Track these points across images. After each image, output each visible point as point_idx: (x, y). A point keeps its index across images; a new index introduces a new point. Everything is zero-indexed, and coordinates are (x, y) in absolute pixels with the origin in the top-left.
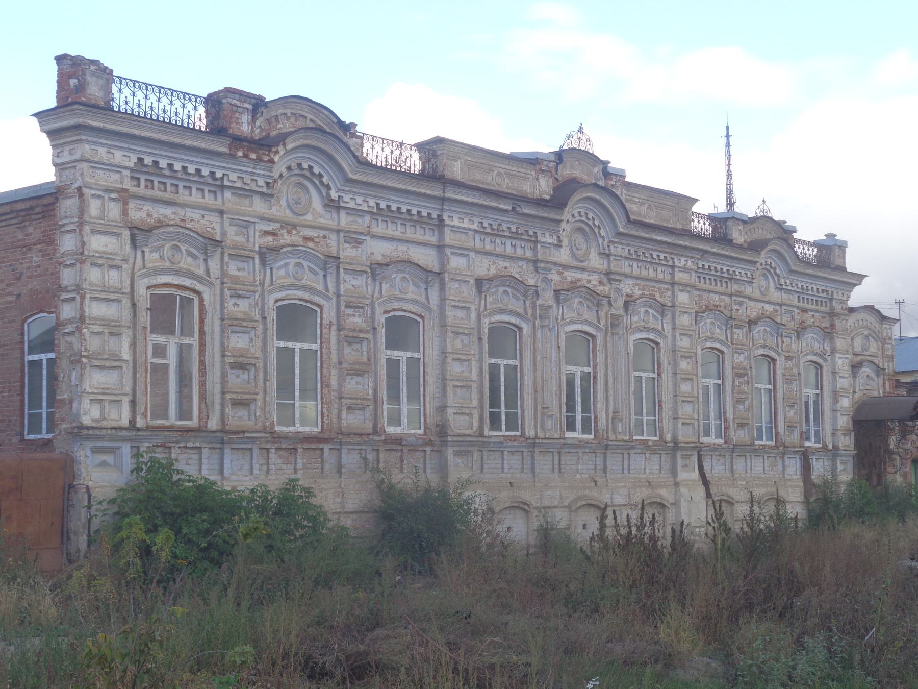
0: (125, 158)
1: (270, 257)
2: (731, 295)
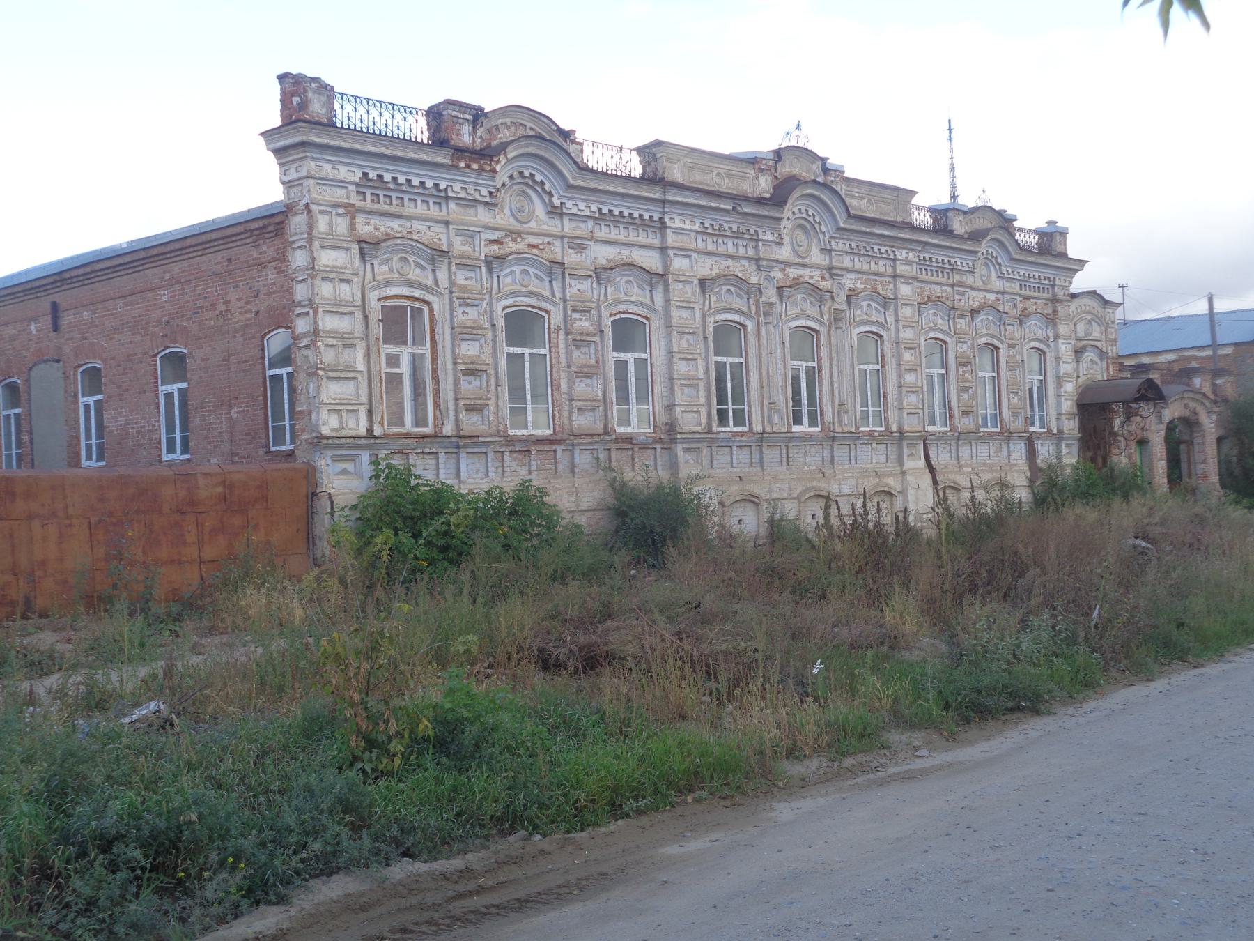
0: (349, 173)
1: (496, 265)
2: (953, 286)
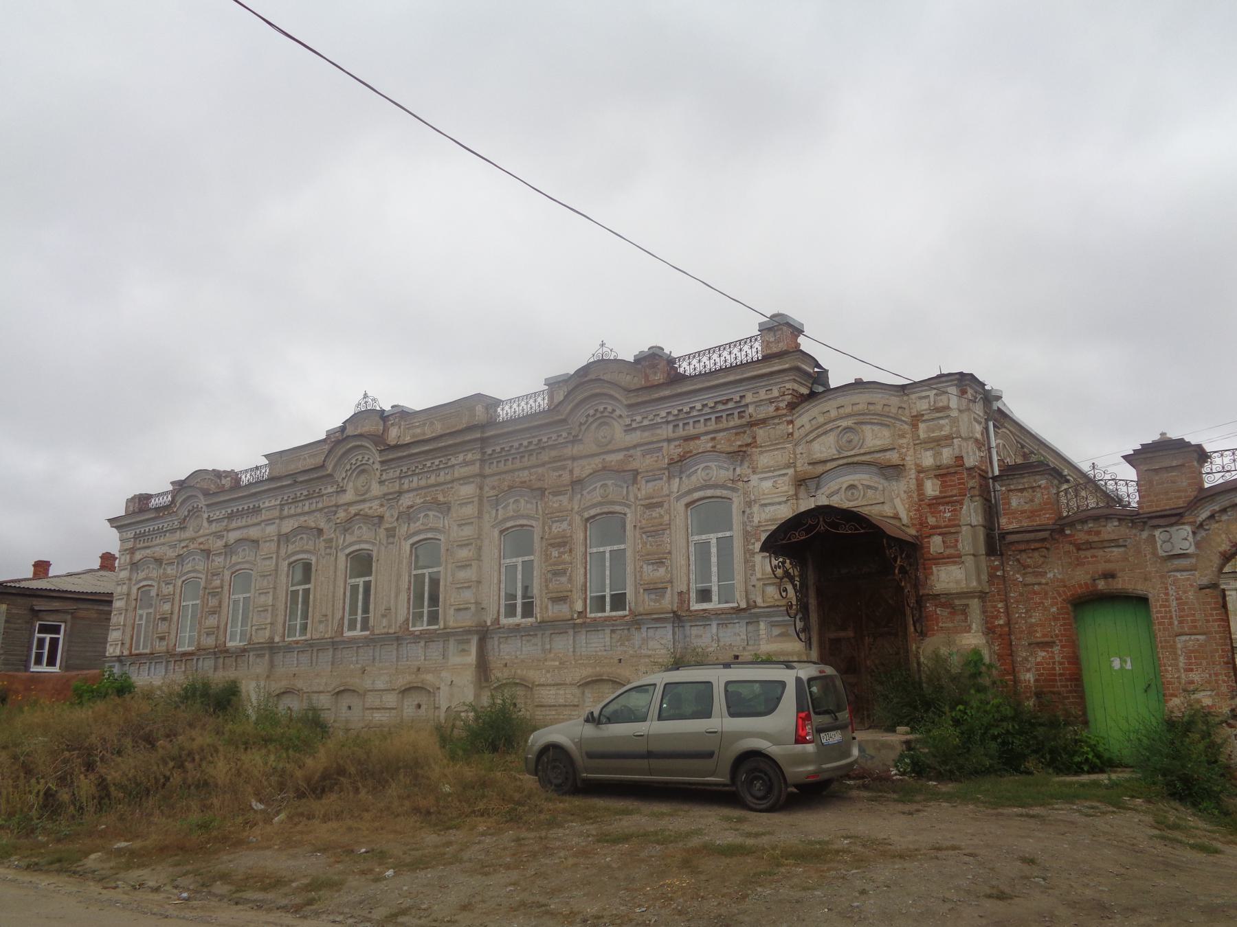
2: (543, 465)
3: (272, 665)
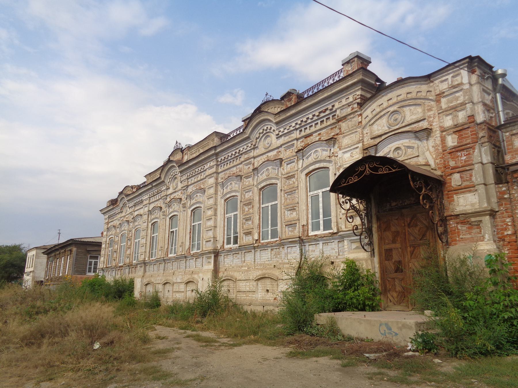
3: (145, 271)
